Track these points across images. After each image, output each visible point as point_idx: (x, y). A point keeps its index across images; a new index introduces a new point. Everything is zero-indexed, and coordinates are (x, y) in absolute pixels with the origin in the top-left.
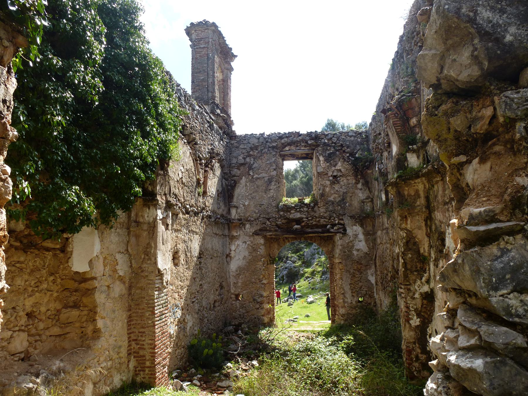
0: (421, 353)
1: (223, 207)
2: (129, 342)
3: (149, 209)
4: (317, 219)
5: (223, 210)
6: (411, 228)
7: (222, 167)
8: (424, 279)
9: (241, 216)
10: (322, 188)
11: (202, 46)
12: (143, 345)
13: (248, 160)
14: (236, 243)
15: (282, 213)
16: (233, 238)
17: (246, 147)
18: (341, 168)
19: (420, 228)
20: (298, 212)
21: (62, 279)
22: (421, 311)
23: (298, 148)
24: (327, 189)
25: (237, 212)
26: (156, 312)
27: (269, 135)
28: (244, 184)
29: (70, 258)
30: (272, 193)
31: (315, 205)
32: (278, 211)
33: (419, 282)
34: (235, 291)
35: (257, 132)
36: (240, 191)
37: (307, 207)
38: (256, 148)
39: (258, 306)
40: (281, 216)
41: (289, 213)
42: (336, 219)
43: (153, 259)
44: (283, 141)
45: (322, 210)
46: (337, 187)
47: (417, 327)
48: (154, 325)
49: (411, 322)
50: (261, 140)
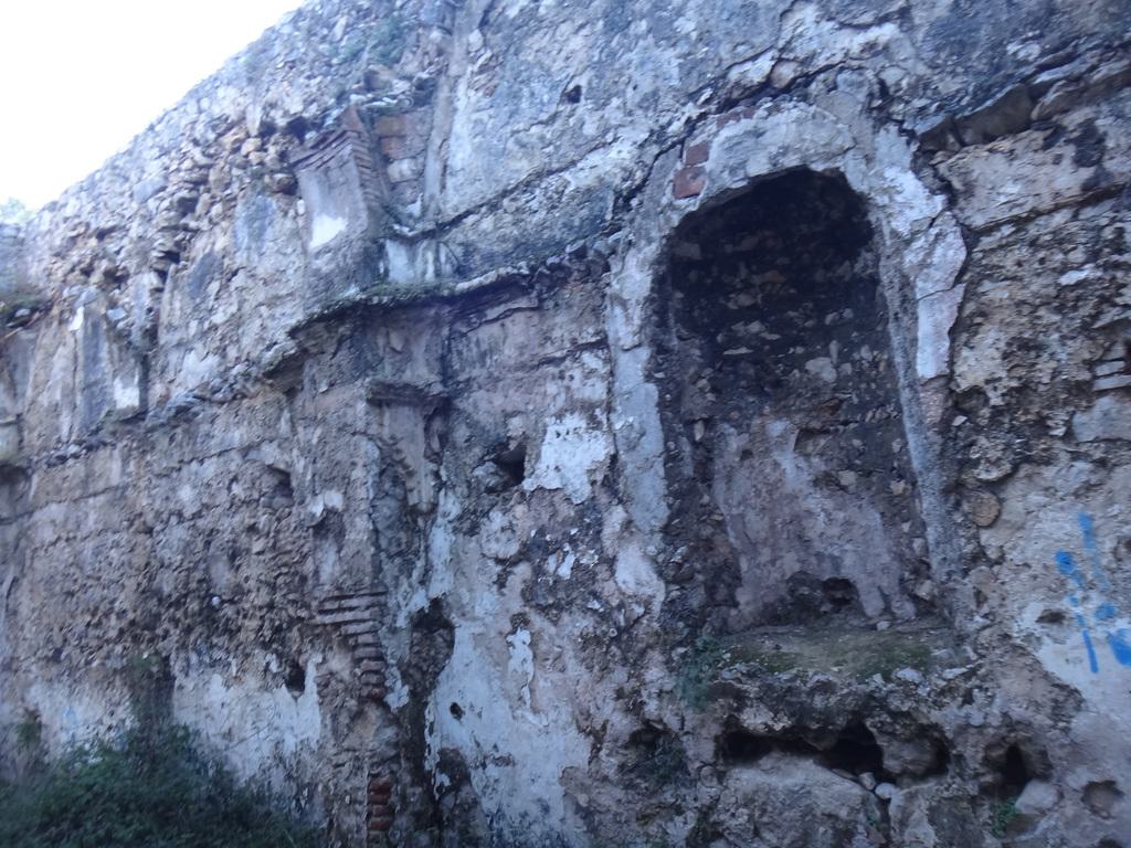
0: (413, 784)
6: (392, 438)
8: (416, 574)
19: (412, 440)
22: (409, 665)
33: (405, 586)
47: (401, 710)
49: (391, 699)
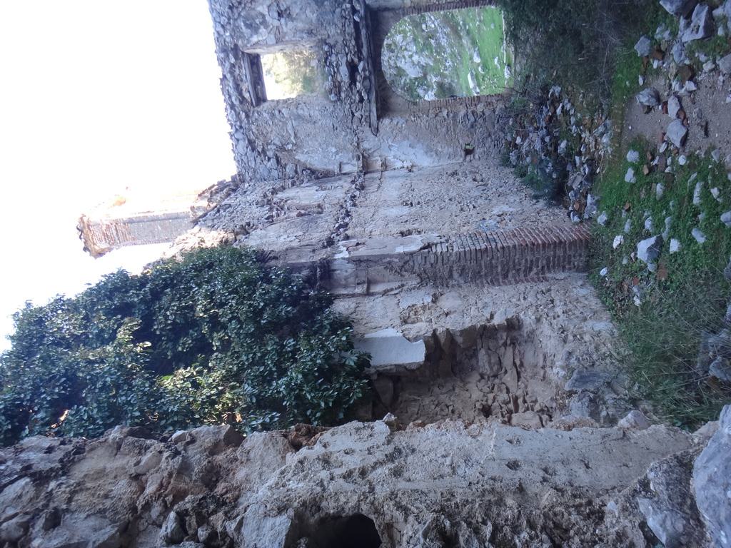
1: (340, 183)
2: (528, 281)
3: (335, 270)
4: (347, 37)
5: (345, 182)
7: (283, 188)
9: (353, 157)
10: (298, 35)
11: (115, 233)
12: (532, 261)
13: (270, 154)
14: (392, 160)
15: (343, 95)
16: (385, 166)
17: (252, 159)
18: (265, 6)
20: (338, 69)
21: (438, 376)
23: (244, 78)
24: (300, 25)
26: (483, 247)
27: (231, 125)
28: (306, 156)
29: (405, 367)
30: (316, 114)
31: (326, 44)
32: (339, 99)
34: (461, 156)
35: (229, 143)
36: (317, 162)
37: (330, 56)
38: (251, 143)
39: (481, 121)
40: (347, 96)
41: (342, 84)
42: (344, 7)
43: (407, 258)
44: (237, 103)
45: (332, 31)
46: (295, 10)
48: (503, 248)
50: (239, 136)
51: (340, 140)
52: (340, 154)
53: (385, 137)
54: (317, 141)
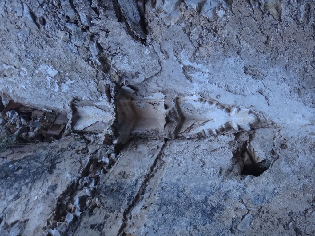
16: (178, 118)
25: (90, 103)
51: (59, 49)
52: (69, 82)
53: (168, 46)
54: (11, 51)
